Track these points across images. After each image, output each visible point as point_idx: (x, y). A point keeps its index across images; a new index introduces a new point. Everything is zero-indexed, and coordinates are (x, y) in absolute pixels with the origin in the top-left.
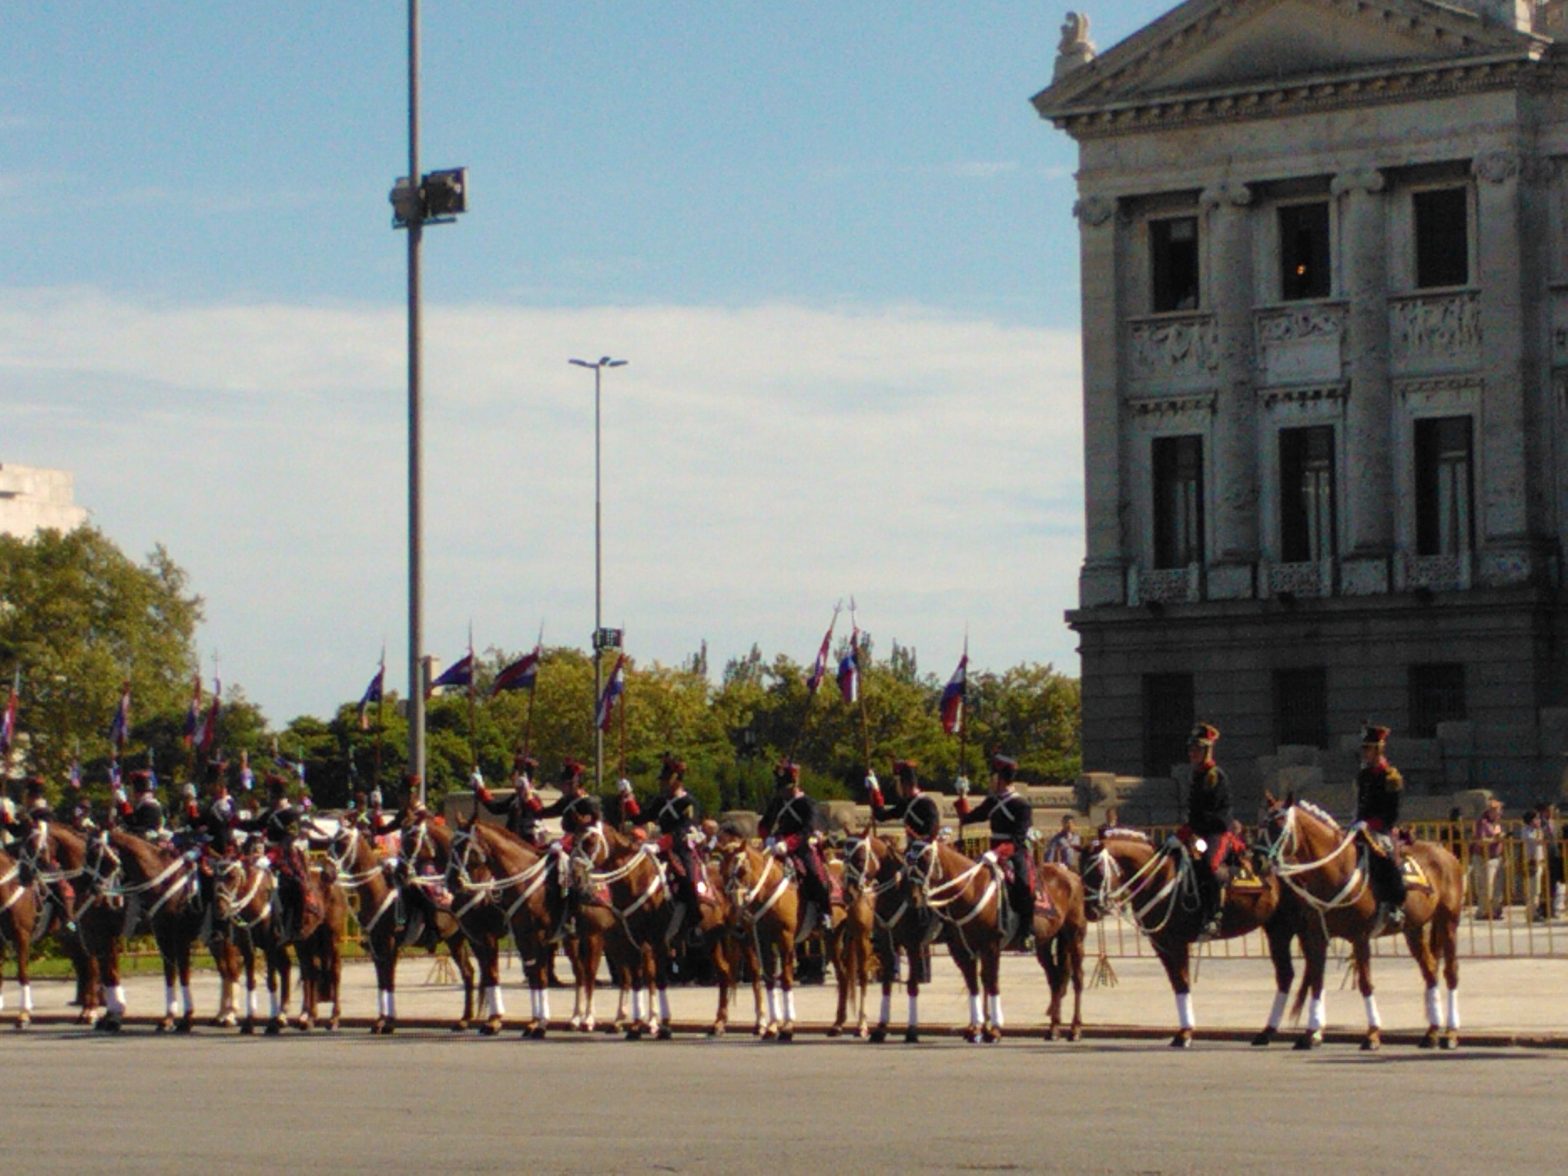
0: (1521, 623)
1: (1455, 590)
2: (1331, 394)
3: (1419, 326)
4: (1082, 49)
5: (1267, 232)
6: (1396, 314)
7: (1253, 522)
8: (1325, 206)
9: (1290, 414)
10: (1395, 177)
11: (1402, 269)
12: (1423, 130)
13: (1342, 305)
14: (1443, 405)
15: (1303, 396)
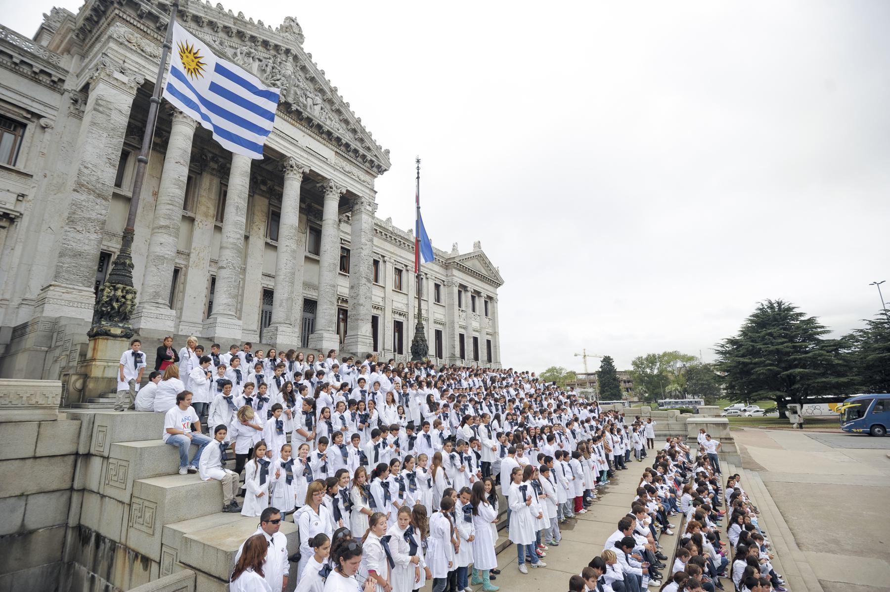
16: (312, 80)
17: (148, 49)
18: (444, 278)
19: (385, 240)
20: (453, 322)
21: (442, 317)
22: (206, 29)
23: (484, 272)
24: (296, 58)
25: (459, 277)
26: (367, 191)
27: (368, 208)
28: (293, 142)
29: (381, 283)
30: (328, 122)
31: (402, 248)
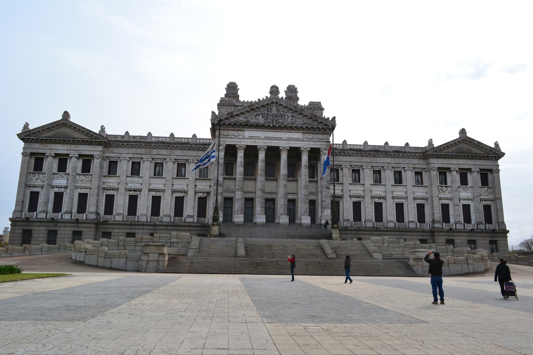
0: (93, 225)
1: (82, 219)
2: (64, 188)
3: (81, 179)
4: (28, 128)
5: (56, 162)
6: (77, 176)
7: (47, 206)
8: (67, 159)
9: (56, 190)
10: (80, 156)
11: (79, 170)
12: (86, 150)
13: (68, 174)
14: (83, 191)
15: (59, 187)
16: (286, 107)
17: (226, 134)
18: (423, 166)
19: (362, 156)
20: (432, 197)
21: (424, 194)
22: (241, 115)
23: (474, 150)
24: (276, 103)
25: (437, 163)
26: (325, 143)
27: (325, 152)
28: (281, 139)
29: (362, 182)
30: (298, 120)
31: (378, 157)
